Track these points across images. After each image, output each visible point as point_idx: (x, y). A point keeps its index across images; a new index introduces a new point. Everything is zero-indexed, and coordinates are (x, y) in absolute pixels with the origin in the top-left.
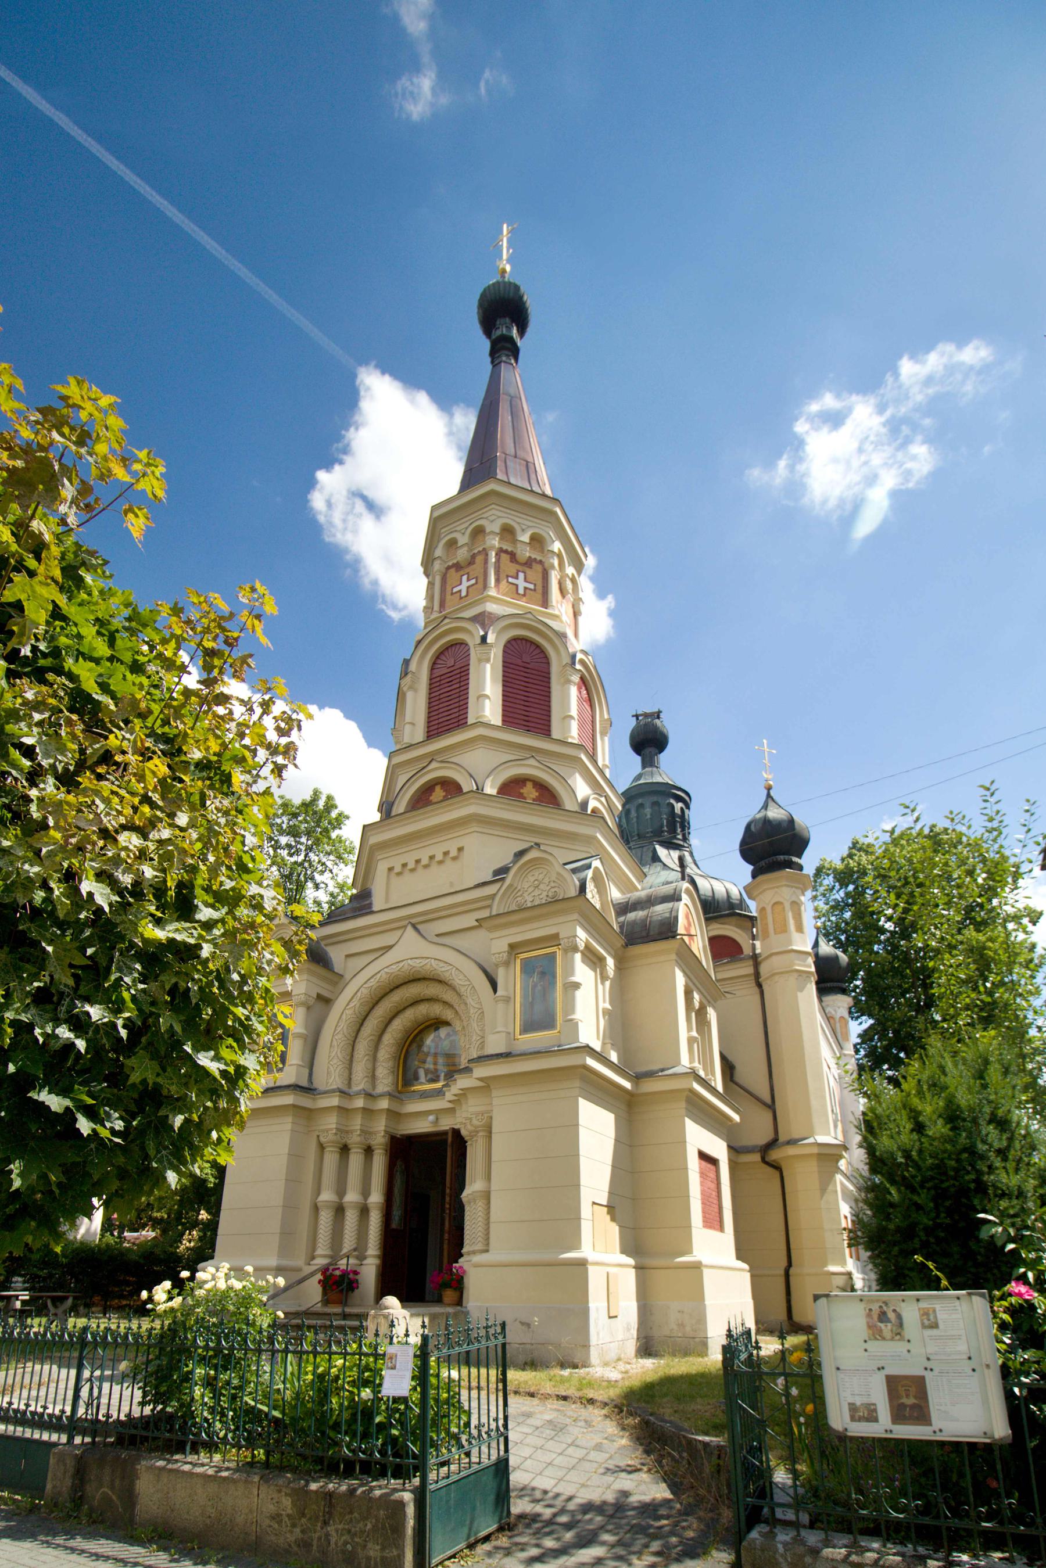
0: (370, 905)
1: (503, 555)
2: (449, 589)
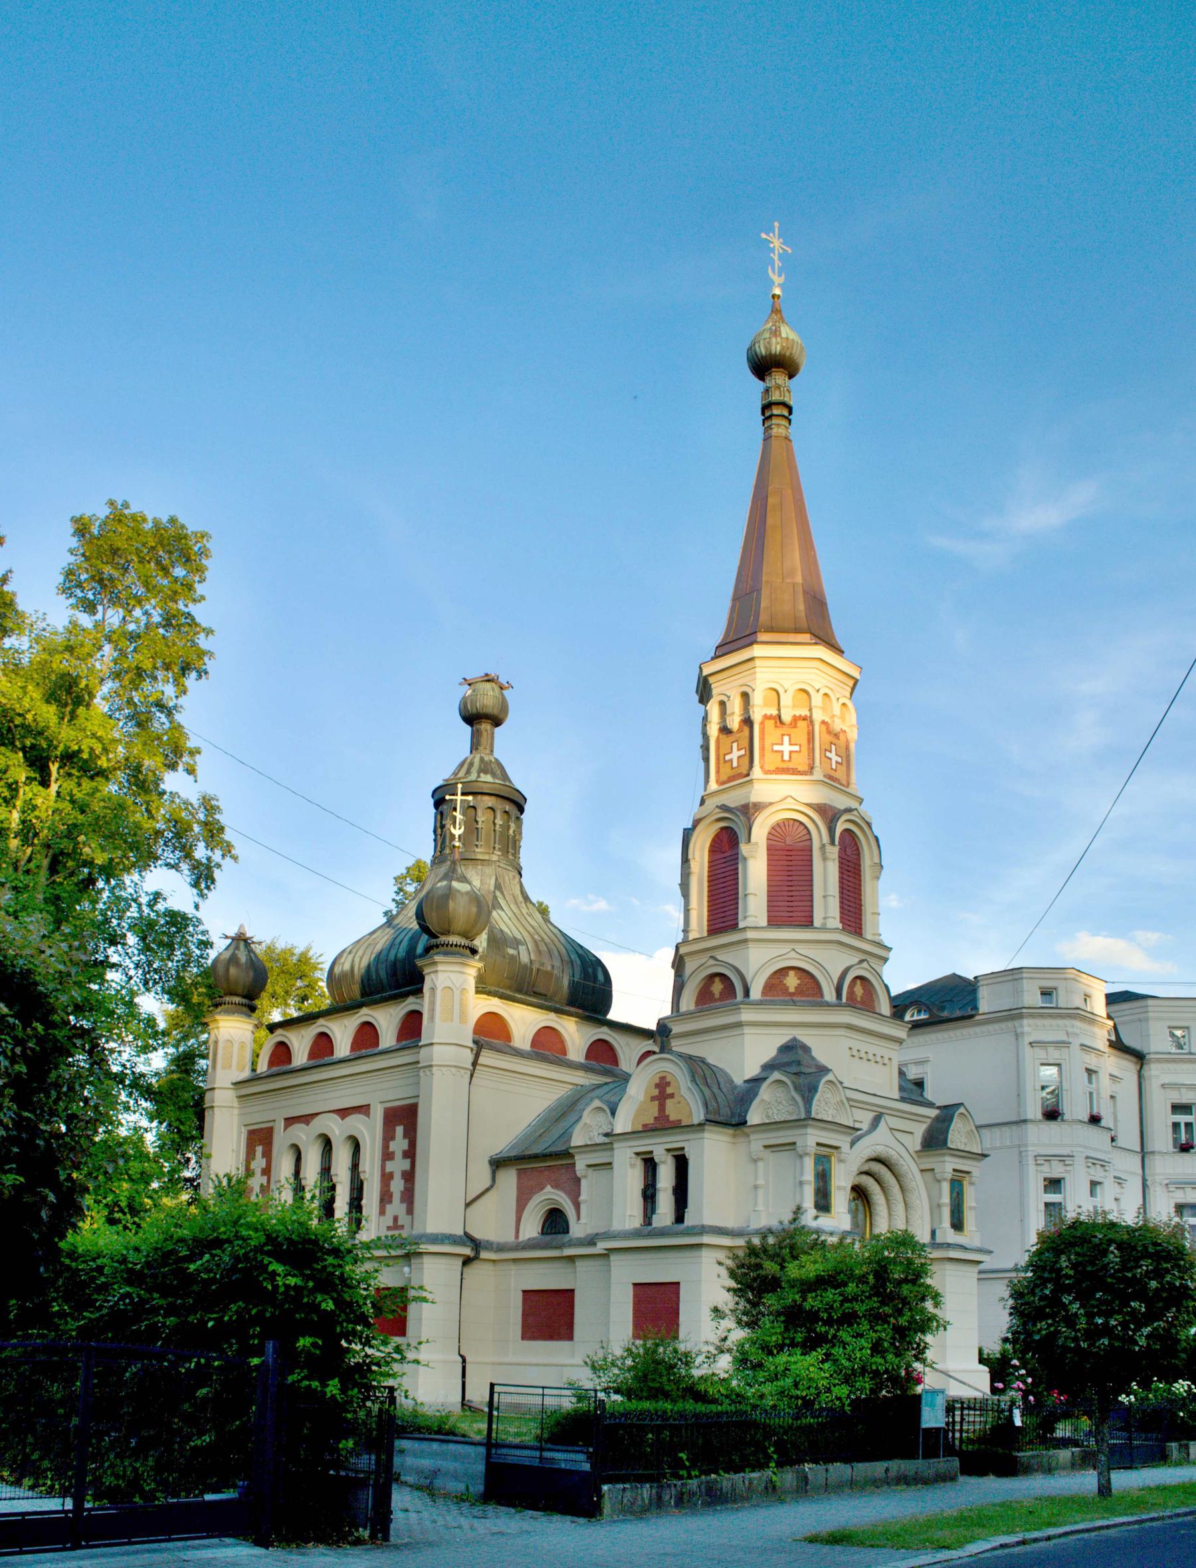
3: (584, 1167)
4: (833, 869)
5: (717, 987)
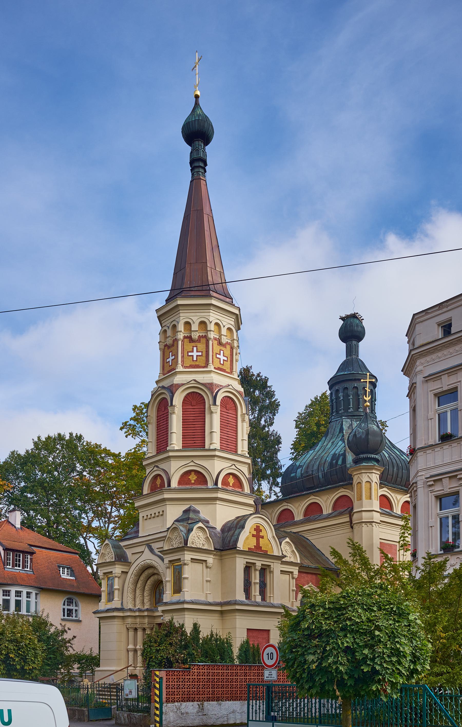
0: (138, 532)
1: (185, 340)
2: (165, 359)
3: (102, 574)
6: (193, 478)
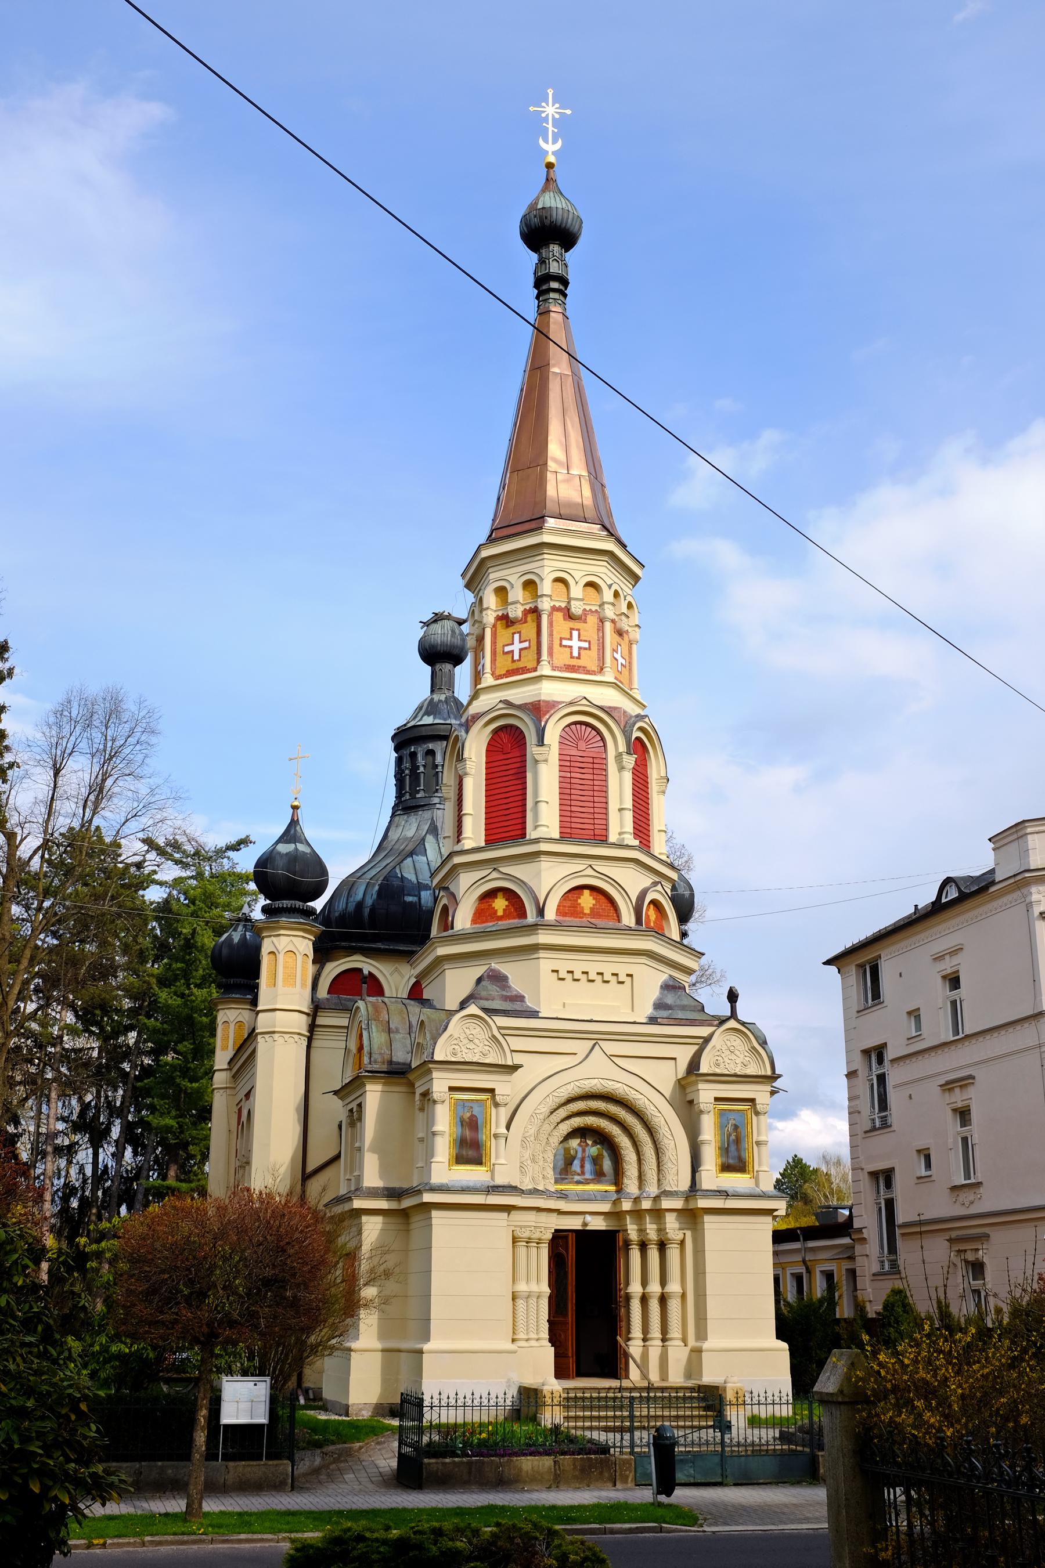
4: (628, 776)
5: (500, 904)
6: (587, 901)
